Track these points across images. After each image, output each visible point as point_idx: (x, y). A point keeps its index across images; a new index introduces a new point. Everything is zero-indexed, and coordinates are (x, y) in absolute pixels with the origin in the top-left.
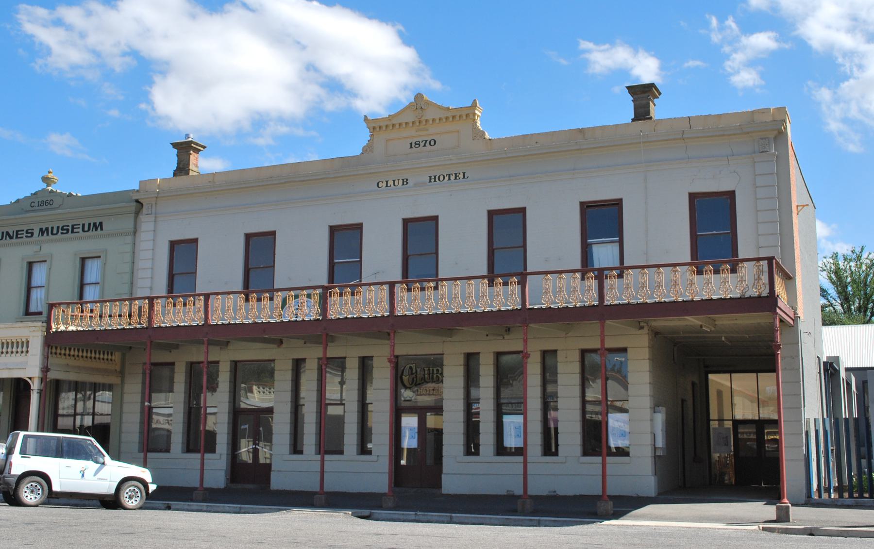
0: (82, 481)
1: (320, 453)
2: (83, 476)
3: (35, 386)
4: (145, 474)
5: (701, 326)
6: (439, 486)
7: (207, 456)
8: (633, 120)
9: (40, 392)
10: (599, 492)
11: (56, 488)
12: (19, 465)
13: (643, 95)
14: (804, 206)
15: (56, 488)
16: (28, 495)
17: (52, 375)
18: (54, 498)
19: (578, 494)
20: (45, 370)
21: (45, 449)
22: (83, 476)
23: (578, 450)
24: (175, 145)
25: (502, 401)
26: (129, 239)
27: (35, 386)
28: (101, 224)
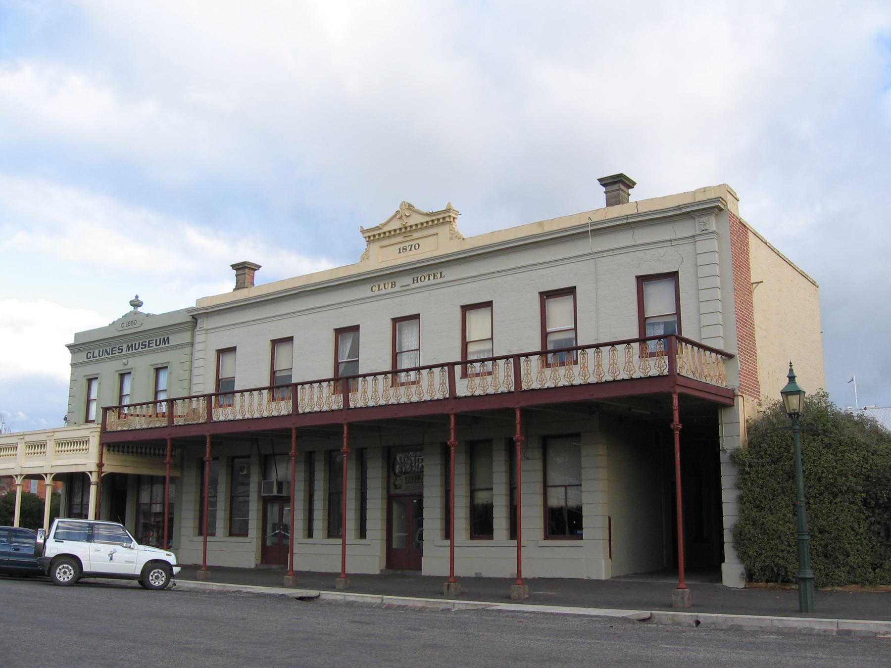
0: (111, 563)
1: (200, 534)
2: (111, 559)
3: (94, 478)
4: (172, 559)
5: (630, 409)
6: (419, 567)
7: (209, 538)
8: (234, 290)
9: (97, 484)
10: (448, 574)
11: (86, 569)
12: (53, 549)
13: (244, 270)
14: (758, 283)
15: (86, 569)
16: (64, 574)
17: (107, 469)
18: (84, 579)
19: (536, 577)
20: (100, 465)
21: (70, 536)
22: (111, 559)
23: (540, 533)
24: (234, 267)
25: (478, 486)
26: (188, 350)
27: (94, 478)
28: (168, 338)
